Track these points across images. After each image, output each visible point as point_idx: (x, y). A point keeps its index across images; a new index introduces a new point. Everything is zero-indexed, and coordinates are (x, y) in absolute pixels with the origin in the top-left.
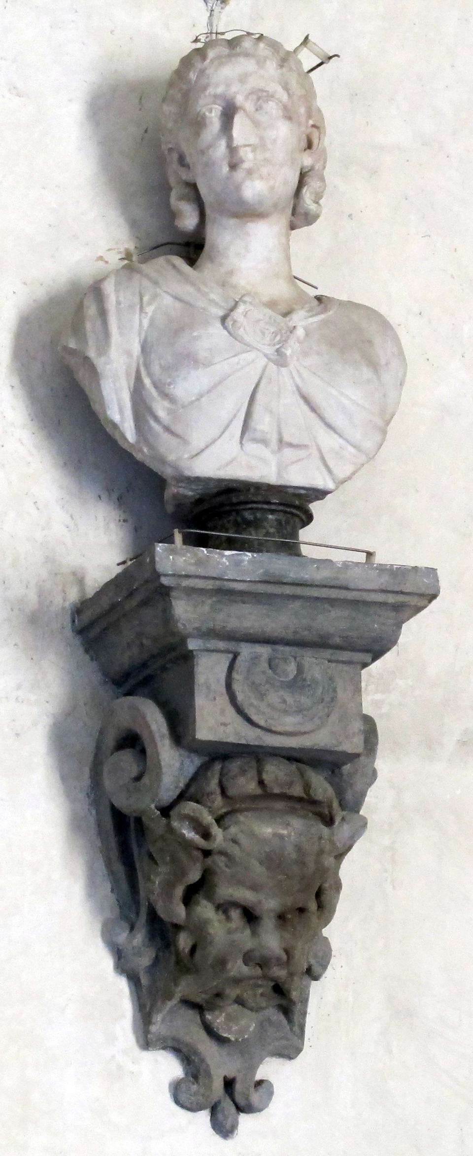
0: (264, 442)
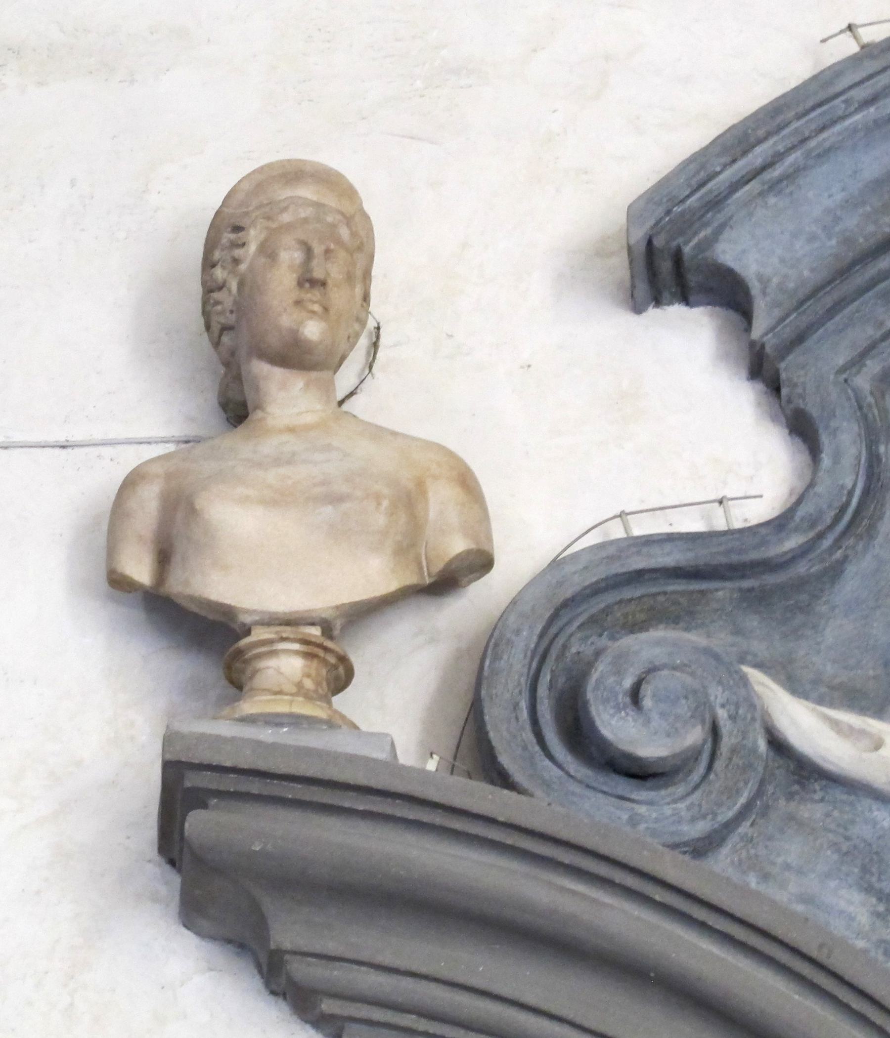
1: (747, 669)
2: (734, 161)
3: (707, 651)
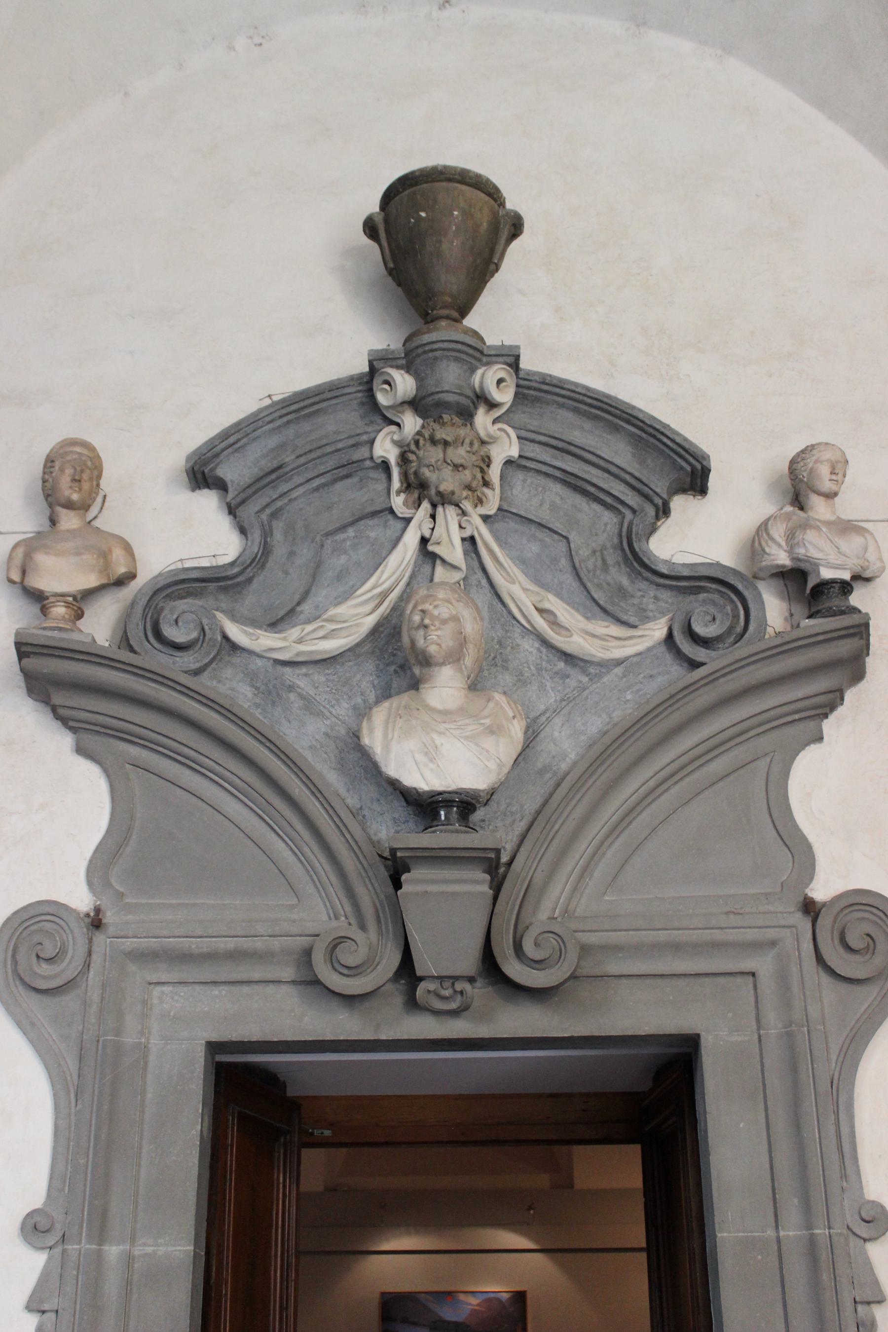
1: (216, 612)
2: (223, 441)
3: (202, 607)
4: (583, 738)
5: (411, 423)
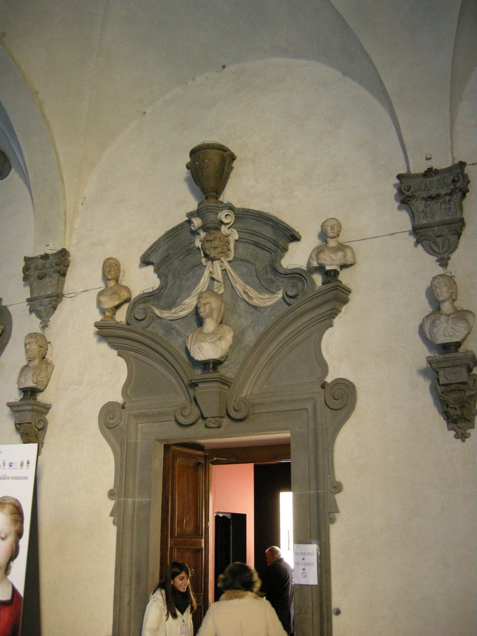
0: (447, 336)
4: (258, 334)
5: (203, 234)
